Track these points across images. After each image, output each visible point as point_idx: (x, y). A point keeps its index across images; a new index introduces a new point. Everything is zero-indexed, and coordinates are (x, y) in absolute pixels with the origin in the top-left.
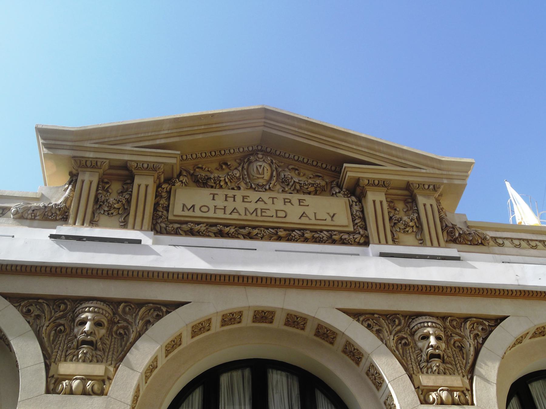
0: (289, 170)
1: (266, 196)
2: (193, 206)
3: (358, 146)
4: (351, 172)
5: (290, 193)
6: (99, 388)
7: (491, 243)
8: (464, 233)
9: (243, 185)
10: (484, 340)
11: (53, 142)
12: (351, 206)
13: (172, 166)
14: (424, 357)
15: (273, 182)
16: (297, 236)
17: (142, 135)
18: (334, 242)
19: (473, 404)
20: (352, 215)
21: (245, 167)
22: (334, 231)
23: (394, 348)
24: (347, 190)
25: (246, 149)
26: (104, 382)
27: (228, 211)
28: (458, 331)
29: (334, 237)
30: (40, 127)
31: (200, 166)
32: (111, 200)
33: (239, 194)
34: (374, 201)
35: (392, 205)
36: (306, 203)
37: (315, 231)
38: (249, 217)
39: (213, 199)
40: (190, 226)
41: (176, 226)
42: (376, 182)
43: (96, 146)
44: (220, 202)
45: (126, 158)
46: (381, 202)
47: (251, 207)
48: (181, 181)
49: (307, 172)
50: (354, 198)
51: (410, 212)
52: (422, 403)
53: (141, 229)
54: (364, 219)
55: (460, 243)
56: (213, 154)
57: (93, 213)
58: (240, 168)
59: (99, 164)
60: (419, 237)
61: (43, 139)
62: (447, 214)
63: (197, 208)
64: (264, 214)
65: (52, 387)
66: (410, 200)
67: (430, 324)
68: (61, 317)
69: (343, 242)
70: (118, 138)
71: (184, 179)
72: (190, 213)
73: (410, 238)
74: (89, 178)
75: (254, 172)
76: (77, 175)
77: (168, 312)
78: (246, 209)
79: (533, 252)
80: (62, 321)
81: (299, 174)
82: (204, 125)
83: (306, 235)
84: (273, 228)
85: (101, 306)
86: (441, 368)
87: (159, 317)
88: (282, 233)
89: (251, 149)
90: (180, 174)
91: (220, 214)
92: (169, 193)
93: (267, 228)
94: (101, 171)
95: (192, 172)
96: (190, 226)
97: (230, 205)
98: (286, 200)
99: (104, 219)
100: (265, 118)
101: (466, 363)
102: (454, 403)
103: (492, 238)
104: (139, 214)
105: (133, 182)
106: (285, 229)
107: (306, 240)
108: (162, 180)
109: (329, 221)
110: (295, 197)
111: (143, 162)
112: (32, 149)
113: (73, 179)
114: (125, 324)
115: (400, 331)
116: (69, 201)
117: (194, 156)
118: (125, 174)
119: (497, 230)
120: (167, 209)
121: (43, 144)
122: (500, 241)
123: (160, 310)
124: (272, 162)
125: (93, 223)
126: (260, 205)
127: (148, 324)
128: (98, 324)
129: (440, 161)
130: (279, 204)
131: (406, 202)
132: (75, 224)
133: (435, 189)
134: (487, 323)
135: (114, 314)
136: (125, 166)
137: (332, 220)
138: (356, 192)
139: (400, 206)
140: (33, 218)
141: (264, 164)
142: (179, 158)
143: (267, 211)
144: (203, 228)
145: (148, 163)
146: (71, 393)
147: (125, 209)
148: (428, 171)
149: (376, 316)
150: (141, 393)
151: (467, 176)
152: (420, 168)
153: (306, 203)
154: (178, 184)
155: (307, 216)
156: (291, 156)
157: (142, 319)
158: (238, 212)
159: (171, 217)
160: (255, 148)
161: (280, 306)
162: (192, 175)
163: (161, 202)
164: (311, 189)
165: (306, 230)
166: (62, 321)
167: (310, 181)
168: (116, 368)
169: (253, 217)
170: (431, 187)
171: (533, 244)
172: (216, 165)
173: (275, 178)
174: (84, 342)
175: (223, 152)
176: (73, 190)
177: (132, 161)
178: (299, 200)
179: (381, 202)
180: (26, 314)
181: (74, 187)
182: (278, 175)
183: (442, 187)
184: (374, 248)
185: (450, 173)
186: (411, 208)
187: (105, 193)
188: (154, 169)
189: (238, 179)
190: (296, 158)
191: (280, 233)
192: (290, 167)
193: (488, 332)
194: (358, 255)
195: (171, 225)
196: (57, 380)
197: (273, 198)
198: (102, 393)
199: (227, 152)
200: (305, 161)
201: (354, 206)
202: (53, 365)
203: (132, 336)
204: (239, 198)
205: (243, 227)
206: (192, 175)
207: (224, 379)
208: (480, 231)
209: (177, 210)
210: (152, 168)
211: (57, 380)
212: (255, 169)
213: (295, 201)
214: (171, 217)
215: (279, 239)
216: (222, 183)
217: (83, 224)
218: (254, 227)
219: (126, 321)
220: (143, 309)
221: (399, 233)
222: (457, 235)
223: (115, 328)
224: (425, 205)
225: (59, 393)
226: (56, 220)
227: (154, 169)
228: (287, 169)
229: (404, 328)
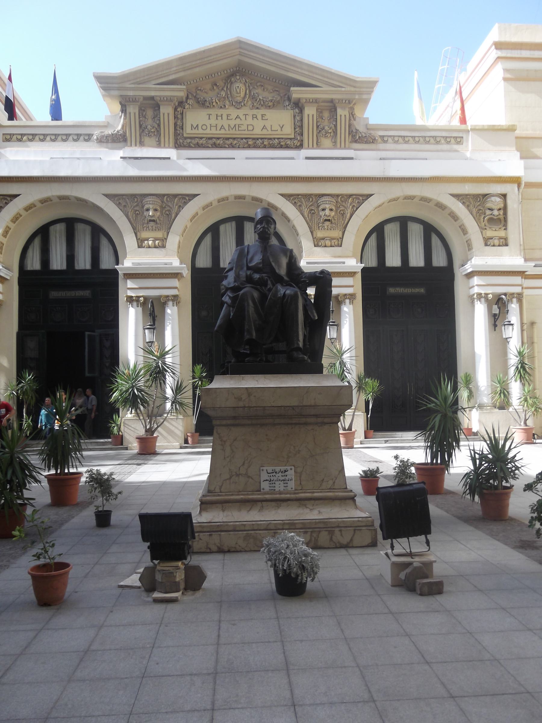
0: (257, 86)
1: (241, 113)
2: (197, 125)
3: (302, 69)
4: (297, 93)
5: (258, 108)
6: (162, 245)
7: (380, 140)
8: (362, 136)
10: (357, 208)
11: (106, 85)
12: (294, 116)
13: (182, 97)
14: (322, 221)
15: (246, 100)
16: (260, 144)
17: (160, 73)
18: (281, 147)
19: (341, 246)
20: (294, 124)
21: (229, 87)
22: (282, 138)
23: (306, 216)
24: (294, 103)
25: (229, 71)
26: (163, 240)
27: (218, 128)
28: (344, 204)
29: (282, 143)
30: (96, 75)
31: (199, 88)
32: (149, 127)
33: (224, 112)
34: (308, 115)
35: (321, 115)
36: (266, 118)
37: (271, 139)
38: (231, 132)
39: (209, 119)
40: (197, 140)
41: (189, 141)
42: (311, 100)
43: (133, 86)
45: (153, 94)
46: (313, 115)
47: (232, 123)
48: (189, 104)
49: (270, 88)
50: (297, 110)
51: (332, 120)
52: (315, 246)
53: (169, 147)
54: (301, 127)
55: (359, 143)
56: (207, 77)
57: (140, 135)
58: (225, 89)
59: (137, 99)
60: (333, 141)
61: (100, 83)
62: (357, 119)
64: (240, 129)
65: (140, 244)
66: (333, 110)
67: (327, 202)
68: (137, 205)
69: (287, 147)
70: (146, 77)
71: (190, 102)
72: (195, 131)
73: (327, 142)
74: (133, 110)
75: (234, 93)
76: (125, 106)
77: (190, 200)
78: (229, 125)
79: (405, 146)
80: (137, 208)
81: (264, 90)
82: (199, 59)
83: (265, 143)
84: (246, 139)
85: (155, 200)
86: (329, 227)
87: (185, 203)
88: (251, 142)
89: (232, 70)
90: (187, 98)
91: (214, 131)
92: (182, 114)
93: (242, 139)
94: (139, 104)
95: (195, 95)
96: (197, 140)
97: (220, 123)
98: (254, 116)
99: (147, 140)
100: (240, 48)
101: (344, 223)
102: (331, 246)
103: (380, 136)
104: (167, 139)
105: (159, 108)
106: (254, 139)
107: (265, 147)
108: (177, 104)
109: (279, 132)
110: (259, 113)
111: (164, 97)
112: (95, 88)
113: (124, 110)
114: (168, 208)
115: (311, 205)
116: (125, 128)
117: (195, 81)
118: (154, 104)
119: (386, 130)
121: (101, 87)
122: (386, 139)
123: (185, 199)
124: (246, 81)
125: (142, 144)
126: (238, 121)
127: (180, 208)
128: (156, 210)
129: (355, 81)
131: (331, 111)
132: (131, 145)
133: (349, 102)
134: (361, 198)
135: (162, 202)
136: (152, 98)
137: (281, 130)
138: (298, 106)
139: (326, 114)
140: (107, 142)
141: (242, 86)
142: (185, 91)
143: (241, 126)
144: (203, 141)
145: (167, 97)
146: (149, 247)
147: (158, 131)
148: (346, 89)
149: (300, 196)
150: (181, 242)
151: (372, 91)
152: (342, 87)
153: (266, 118)
154: (187, 106)
155: (266, 128)
156: (259, 75)
157: (176, 205)
158: (224, 128)
159: (185, 135)
160: (235, 69)
161: (247, 194)
162: (195, 97)
163: (178, 124)
164: (270, 104)
165: (265, 138)
166: (137, 208)
167: (270, 98)
168: (168, 233)
169: (233, 132)
170: (347, 101)
171: (407, 139)
172: (209, 86)
173: (248, 96)
174: (151, 221)
175: (213, 76)
176: (124, 119)
177: (156, 96)
178: (262, 115)
179: (313, 115)
180: (118, 205)
181: (125, 115)
182: (250, 92)
183: (354, 102)
184: (304, 153)
185: (361, 90)
186: (333, 116)
187: (144, 119)
188: (171, 101)
189: (224, 98)
190: (262, 76)
191: (249, 143)
192: (258, 84)
193: (360, 204)
194: (293, 158)
195: (185, 141)
196: (141, 240)
197: (246, 115)
198: (164, 246)
199: (216, 75)
200: (268, 78)
201: (297, 117)
202: (138, 233)
203: (173, 216)
204: (225, 117)
205: (228, 139)
206: (195, 97)
207: (222, 228)
208: (372, 132)
209: (188, 131)
210: (169, 100)
211: (141, 240)
212: (235, 89)
213: (259, 117)
214: (185, 135)
215: (249, 147)
216: (214, 104)
217: (136, 146)
218: (234, 139)
219: (169, 206)
220: (176, 199)
221: (322, 138)
222: (357, 138)
223: (164, 211)
224: (341, 116)
225: (144, 247)
226: (120, 142)
227: (171, 101)
228: (256, 87)
229: (314, 203)
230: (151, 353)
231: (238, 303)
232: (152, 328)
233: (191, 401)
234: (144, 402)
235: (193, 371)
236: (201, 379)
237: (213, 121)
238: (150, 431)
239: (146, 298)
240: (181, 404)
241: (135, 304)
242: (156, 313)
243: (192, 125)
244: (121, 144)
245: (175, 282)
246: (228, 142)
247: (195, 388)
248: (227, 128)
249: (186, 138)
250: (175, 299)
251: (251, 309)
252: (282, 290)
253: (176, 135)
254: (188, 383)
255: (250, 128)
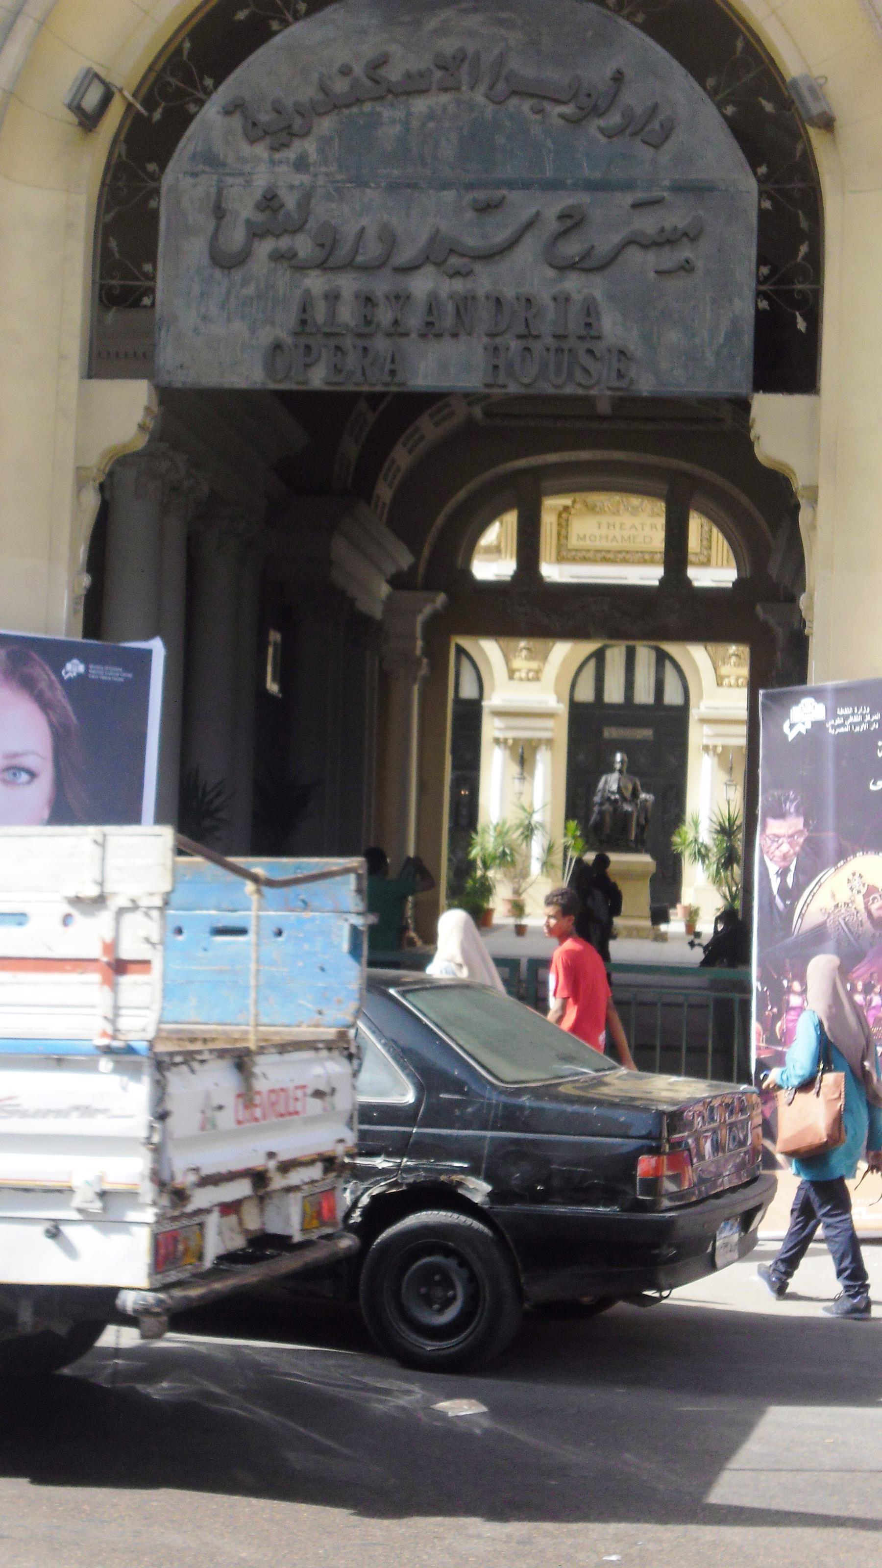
1: (637, 521)
2: (585, 536)
9: (622, 507)
33: (617, 520)
40: (584, 554)
41: (574, 553)
44: (603, 531)
47: (626, 534)
63: (587, 538)
78: (622, 537)
88: (647, 557)
92: (567, 520)
93: (637, 552)
106: (651, 552)
120: (567, 538)
126: (633, 532)
130: (647, 531)
144: (590, 555)
154: (573, 511)
159: (570, 547)
198: (537, 679)
204: (618, 526)
205: (619, 552)
209: (574, 542)
218: (628, 552)
230: (524, 809)
231: (601, 813)
232: (522, 778)
233: (560, 863)
234: (513, 863)
235: (566, 828)
236: (574, 837)
237: (603, 531)
238: (517, 892)
239: (515, 740)
240: (552, 866)
241: (502, 746)
242: (526, 756)
243: (578, 536)
244: (494, 556)
245: (549, 723)
246: (621, 556)
247: (566, 849)
248: (619, 538)
249: (570, 550)
250: (549, 742)
251: (608, 819)
252: (628, 808)
253: (559, 546)
254: (560, 842)
255: (648, 540)
